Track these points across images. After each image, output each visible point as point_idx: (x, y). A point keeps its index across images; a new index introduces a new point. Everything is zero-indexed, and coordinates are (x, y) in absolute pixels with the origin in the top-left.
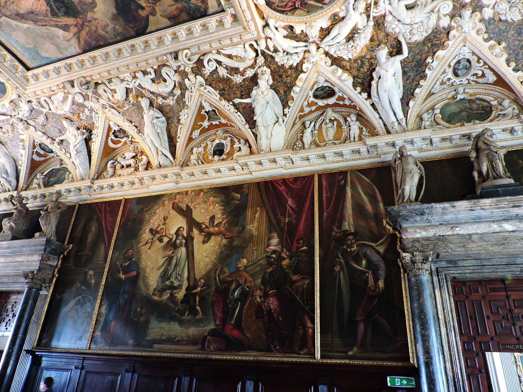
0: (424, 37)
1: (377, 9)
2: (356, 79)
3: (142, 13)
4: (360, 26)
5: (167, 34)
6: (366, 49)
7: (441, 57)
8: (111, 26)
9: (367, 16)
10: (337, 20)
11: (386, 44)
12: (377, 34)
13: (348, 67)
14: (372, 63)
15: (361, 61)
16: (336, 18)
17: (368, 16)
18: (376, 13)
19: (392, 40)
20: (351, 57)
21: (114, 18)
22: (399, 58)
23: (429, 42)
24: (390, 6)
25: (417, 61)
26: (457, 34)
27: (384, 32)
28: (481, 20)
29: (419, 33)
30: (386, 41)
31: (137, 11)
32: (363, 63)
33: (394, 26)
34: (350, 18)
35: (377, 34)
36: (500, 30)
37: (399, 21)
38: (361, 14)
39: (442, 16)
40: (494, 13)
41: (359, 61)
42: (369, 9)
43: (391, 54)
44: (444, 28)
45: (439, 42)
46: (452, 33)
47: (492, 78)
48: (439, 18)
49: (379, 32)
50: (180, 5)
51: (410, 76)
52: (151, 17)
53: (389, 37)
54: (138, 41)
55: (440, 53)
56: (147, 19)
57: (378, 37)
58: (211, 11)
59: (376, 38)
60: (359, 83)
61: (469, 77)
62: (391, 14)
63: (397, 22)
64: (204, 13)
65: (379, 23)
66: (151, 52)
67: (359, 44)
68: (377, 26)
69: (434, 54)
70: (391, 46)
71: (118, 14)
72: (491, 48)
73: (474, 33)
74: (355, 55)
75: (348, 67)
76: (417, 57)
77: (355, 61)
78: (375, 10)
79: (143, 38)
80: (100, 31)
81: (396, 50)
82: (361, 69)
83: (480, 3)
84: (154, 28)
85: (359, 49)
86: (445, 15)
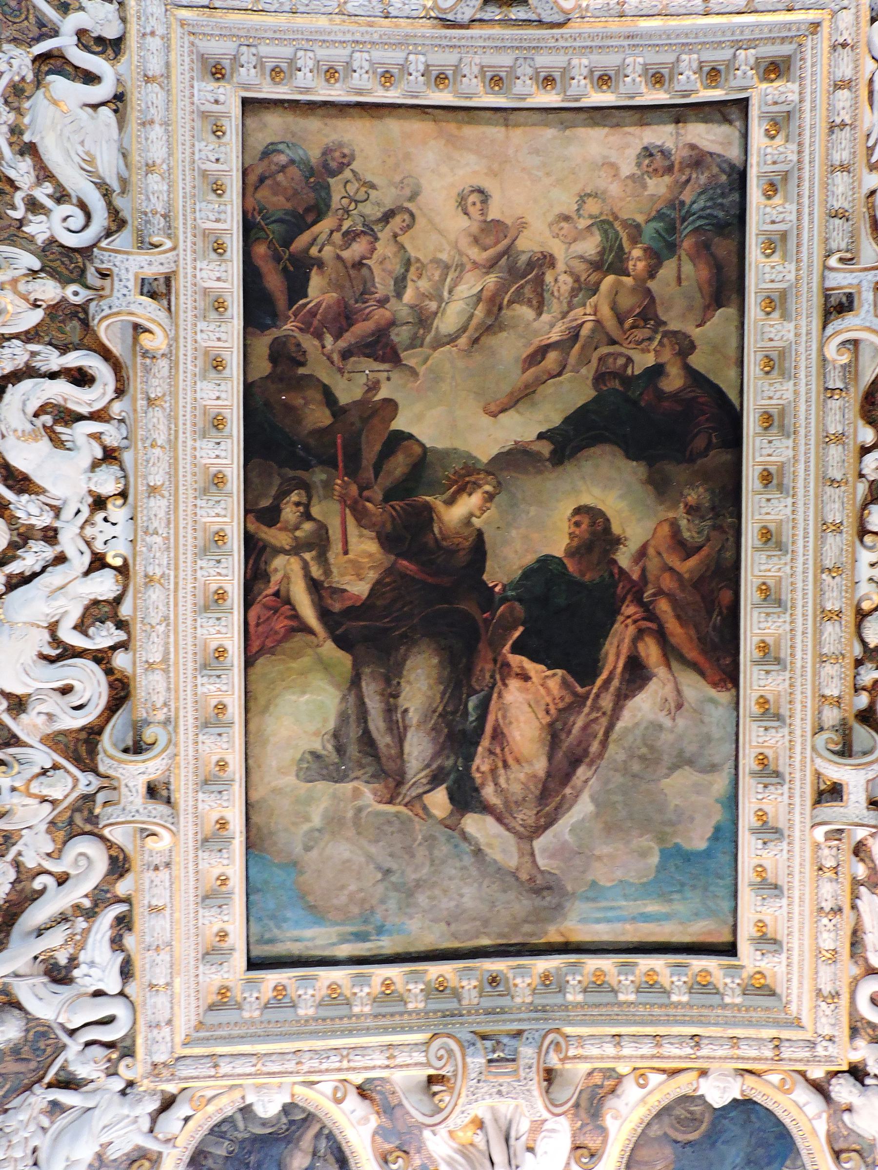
3: (674, 381)
5: (763, 330)
8: (680, 513)
21: (660, 486)
31: (661, 395)
50: (686, 244)
52: (697, 361)
54: (758, 451)
56: (695, 377)
58: (733, 153)
64: (735, 176)
66: (802, 407)
71: (650, 465)
79: (751, 424)
80: (688, 566)
84: (733, 373)
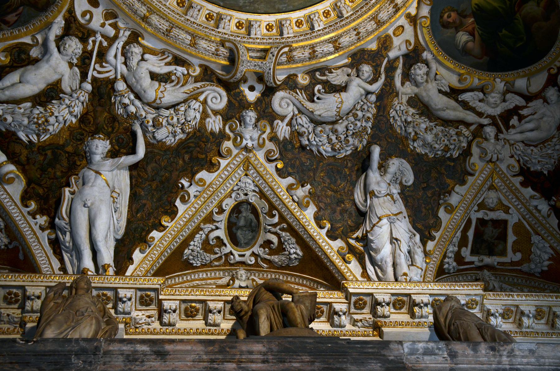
0: (177, 138)
1: (102, 66)
2: (33, 185)
4: (66, 86)
6: (68, 133)
7: (207, 183)
9: (81, 73)
10: (23, 60)
11: (108, 136)
12: (95, 111)
13: (23, 158)
14: (75, 162)
15: (54, 153)
16: (23, 56)
17: (84, 76)
18: (99, 72)
19: (121, 130)
20: (34, 138)
22: (131, 160)
23: (187, 152)
24: (124, 67)
25: (162, 182)
26: (235, 152)
27: (109, 112)
28: (273, 138)
29: (170, 128)
30: (110, 130)
32: (56, 159)
33: (126, 101)
34: (48, 61)
35: (95, 111)
36: (302, 164)
37: (138, 97)
38: (71, 65)
39: (210, 112)
40: (292, 133)
41: (49, 153)
42: (87, 61)
43: (113, 154)
44: (212, 133)
45: (204, 156)
46: (228, 144)
47: (295, 250)
48: (205, 115)
49: (99, 109)
51: (145, 205)
53: (116, 124)
55: (203, 174)
57: (95, 118)
59: (92, 120)
60: (38, 195)
61: (256, 249)
62: (126, 82)
63: (132, 97)
65: (103, 91)
67: (56, 114)
68: (97, 98)
69: (194, 174)
70: (117, 141)
72: (290, 188)
73: (260, 155)
74: (44, 138)
75: (23, 158)
76: (162, 173)
77: (42, 148)
78: (97, 67)
81: (123, 145)
82: (50, 170)
83: (270, 110)
85: (54, 128)
86: (216, 113)
